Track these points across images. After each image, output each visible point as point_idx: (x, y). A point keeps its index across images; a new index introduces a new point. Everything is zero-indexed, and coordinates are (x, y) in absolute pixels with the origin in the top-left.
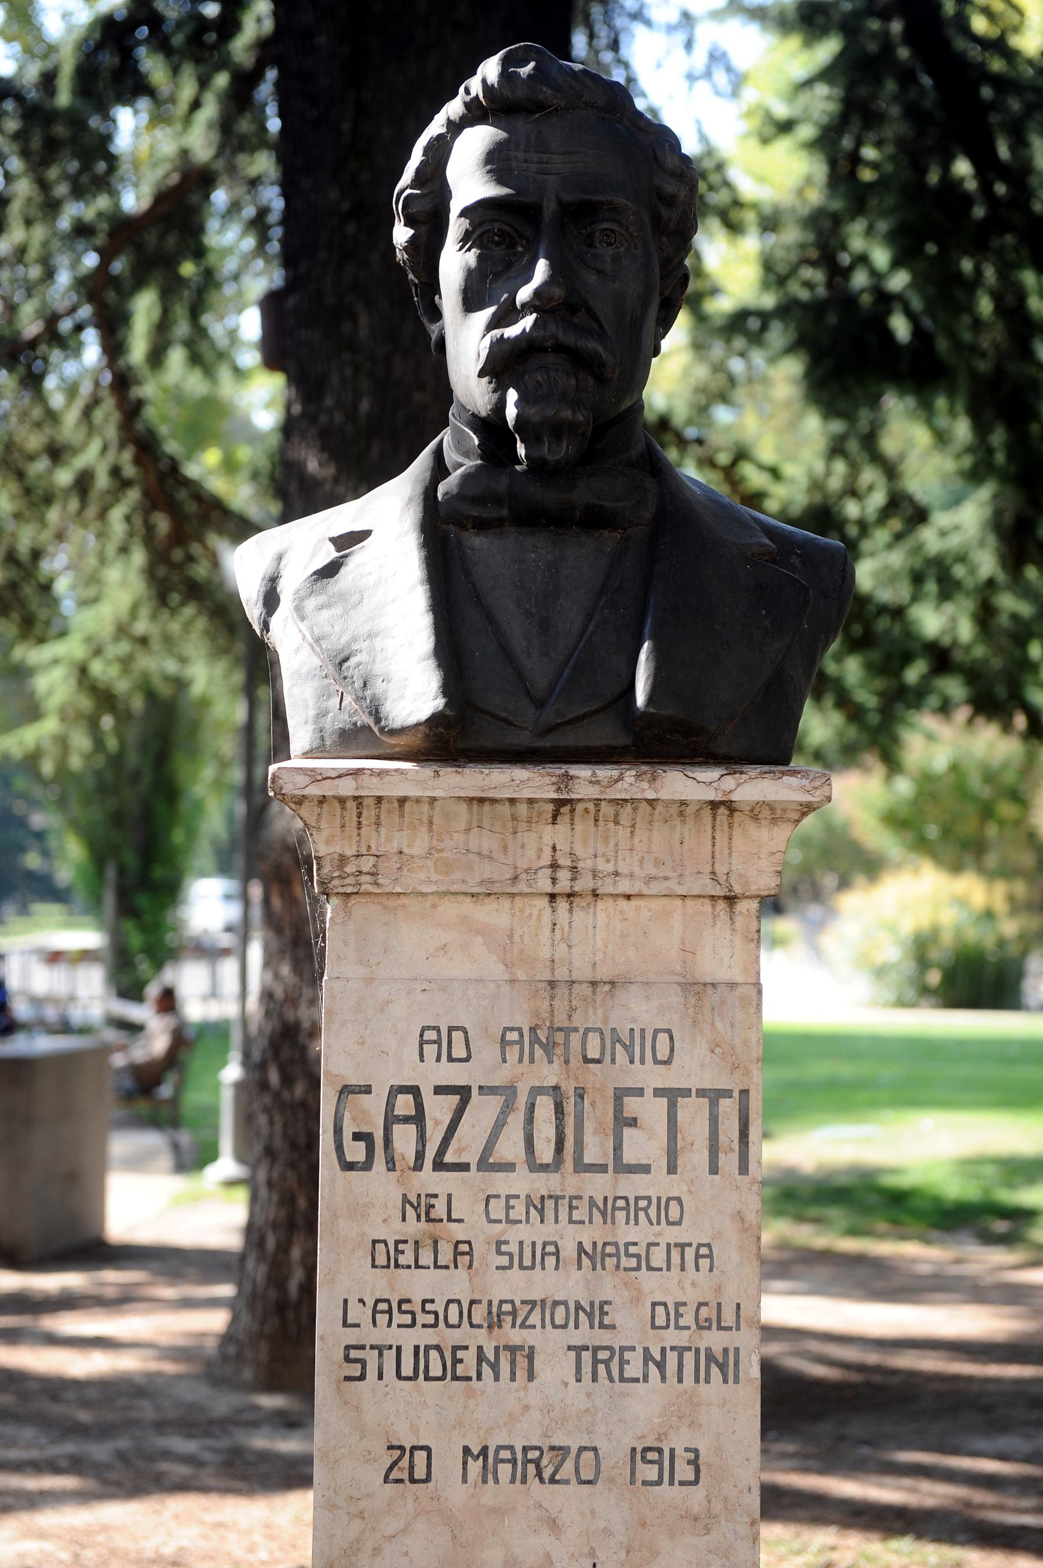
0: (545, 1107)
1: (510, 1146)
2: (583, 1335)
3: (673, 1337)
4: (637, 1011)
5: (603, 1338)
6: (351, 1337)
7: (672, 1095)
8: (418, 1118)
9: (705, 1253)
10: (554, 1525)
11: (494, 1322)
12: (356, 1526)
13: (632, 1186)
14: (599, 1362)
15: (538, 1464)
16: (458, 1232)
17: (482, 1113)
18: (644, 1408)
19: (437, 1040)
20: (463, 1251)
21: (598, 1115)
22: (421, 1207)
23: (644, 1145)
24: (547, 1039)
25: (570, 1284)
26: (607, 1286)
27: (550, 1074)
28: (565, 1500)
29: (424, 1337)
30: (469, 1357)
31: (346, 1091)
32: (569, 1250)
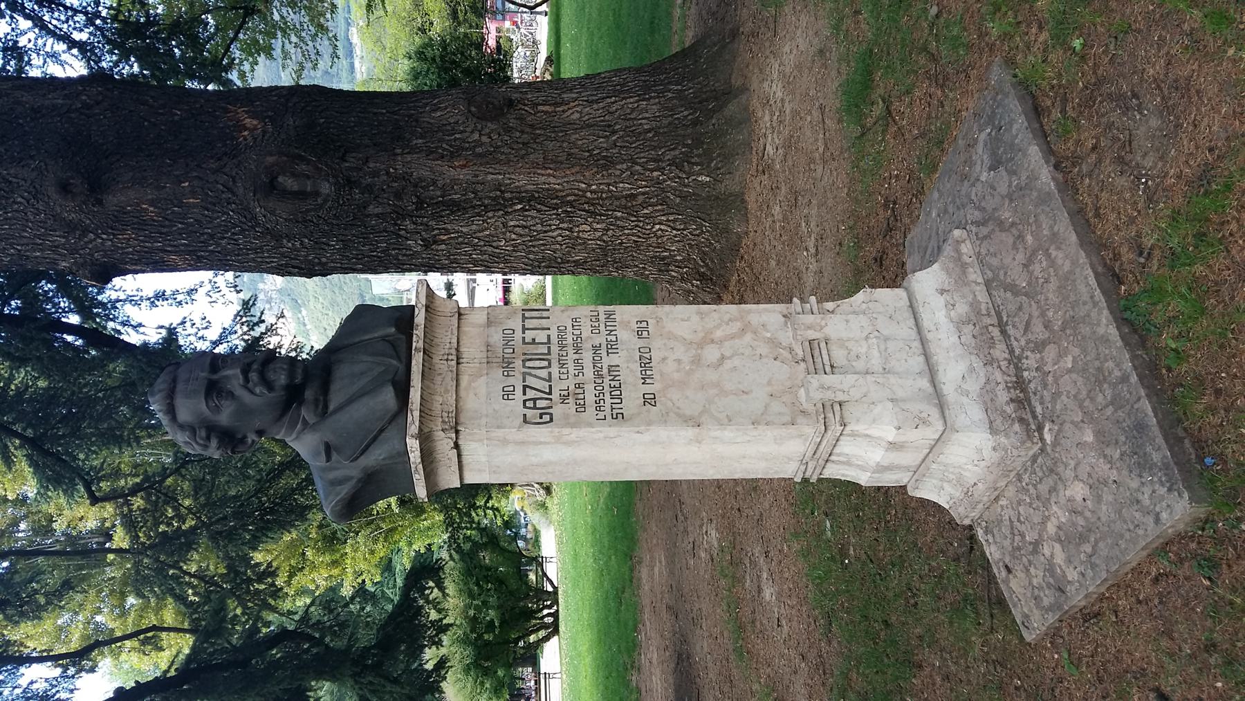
0: (528, 364)
1: (544, 373)
2: (603, 352)
3: (602, 328)
4: (497, 338)
5: (604, 346)
6: (609, 417)
7: (524, 329)
8: (535, 400)
9: (575, 320)
10: (664, 359)
11: (601, 376)
12: (671, 414)
13: (554, 339)
14: (611, 348)
15: (646, 364)
16: (572, 387)
17: (531, 381)
18: (625, 335)
19: (507, 395)
20: (578, 386)
21: (531, 349)
22: (564, 399)
23: (541, 337)
24: (507, 365)
25: (587, 357)
26: (587, 345)
27: (518, 363)
28: (655, 355)
29: (607, 396)
30: (613, 383)
31: (525, 421)
32: (576, 356)
